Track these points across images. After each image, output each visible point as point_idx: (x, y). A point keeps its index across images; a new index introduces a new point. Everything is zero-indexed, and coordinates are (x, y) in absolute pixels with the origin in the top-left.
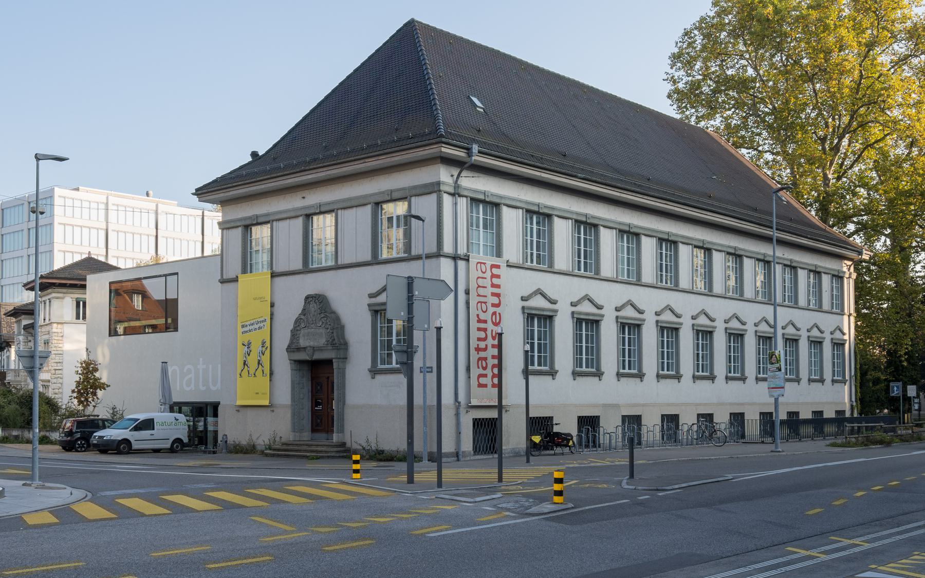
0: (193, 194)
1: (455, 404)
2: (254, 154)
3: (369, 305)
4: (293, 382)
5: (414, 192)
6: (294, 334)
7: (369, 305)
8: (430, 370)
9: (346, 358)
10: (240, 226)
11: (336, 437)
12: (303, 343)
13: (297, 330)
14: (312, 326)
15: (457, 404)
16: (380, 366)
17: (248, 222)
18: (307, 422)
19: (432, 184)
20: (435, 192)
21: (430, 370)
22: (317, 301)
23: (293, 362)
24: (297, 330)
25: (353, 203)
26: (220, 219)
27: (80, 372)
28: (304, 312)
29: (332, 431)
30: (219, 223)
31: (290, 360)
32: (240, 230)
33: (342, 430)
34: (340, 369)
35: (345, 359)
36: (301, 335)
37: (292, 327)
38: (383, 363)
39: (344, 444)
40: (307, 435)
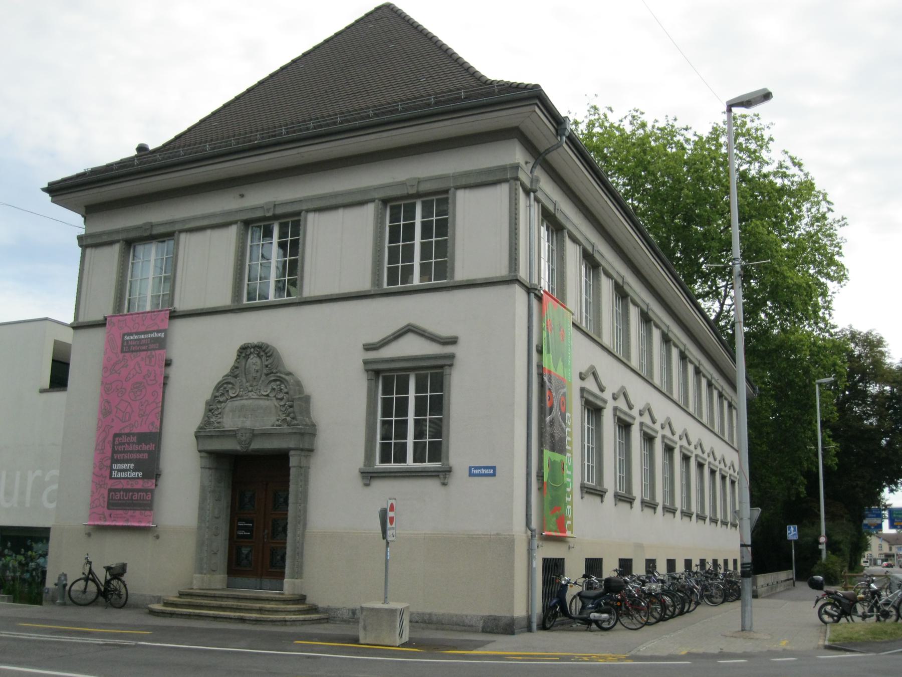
0: (45, 190)
1: (526, 533)
2: (142, 149)
3: (366, 362)
4: (203, 489)
5: (464, 182)
6: (213, 407)
7: (366, 362)
8: (491, 471)
9: (311, 450)
10: (118, 241)
11: (289, 586)
12: (229, 422)
13: (220, 402)
14: (250, 394)
15: (529, 532)
16: (379, 465)
17: (132, 235)
18: (221, 560)
19: (503, 169)
20: (506, 181)
21: (491, 471)
22: (262, 353)
23: (204, 454)
24: (220, 402)
25: (340, 201)
26: (82, 232)
27: (657, 125)
28: (235, 373)
29: (282, 575)
30: (80, 238)
31: (200, 451)
32: (117, 248)
33: (298, 573)
34: (301, 467)
35: (309, 451)
36: (227, 409)
37: (208, 396)
38: (385, 459)
39: (302, 599)
40: (218, 581)
